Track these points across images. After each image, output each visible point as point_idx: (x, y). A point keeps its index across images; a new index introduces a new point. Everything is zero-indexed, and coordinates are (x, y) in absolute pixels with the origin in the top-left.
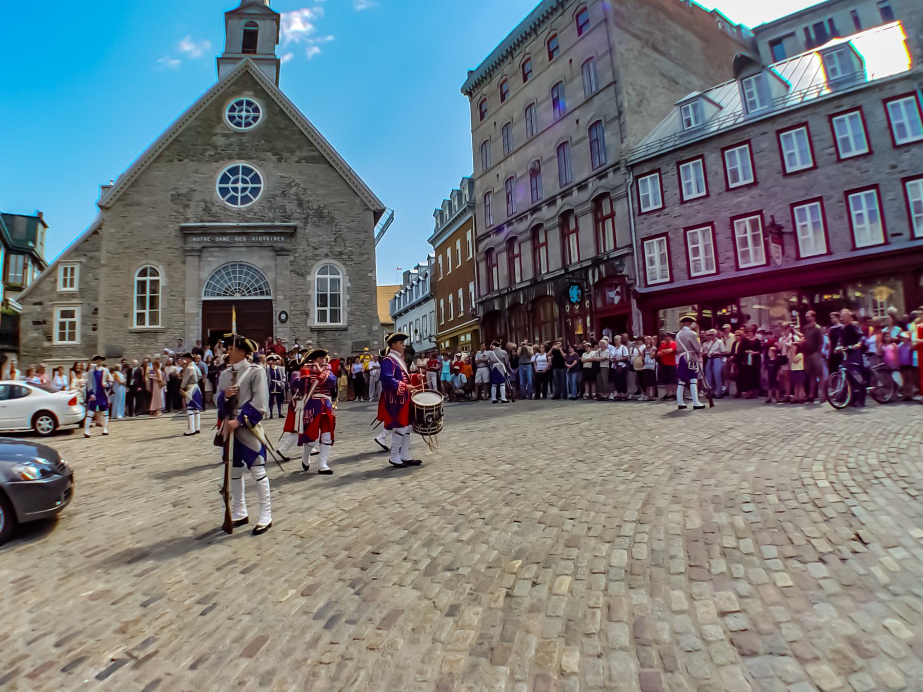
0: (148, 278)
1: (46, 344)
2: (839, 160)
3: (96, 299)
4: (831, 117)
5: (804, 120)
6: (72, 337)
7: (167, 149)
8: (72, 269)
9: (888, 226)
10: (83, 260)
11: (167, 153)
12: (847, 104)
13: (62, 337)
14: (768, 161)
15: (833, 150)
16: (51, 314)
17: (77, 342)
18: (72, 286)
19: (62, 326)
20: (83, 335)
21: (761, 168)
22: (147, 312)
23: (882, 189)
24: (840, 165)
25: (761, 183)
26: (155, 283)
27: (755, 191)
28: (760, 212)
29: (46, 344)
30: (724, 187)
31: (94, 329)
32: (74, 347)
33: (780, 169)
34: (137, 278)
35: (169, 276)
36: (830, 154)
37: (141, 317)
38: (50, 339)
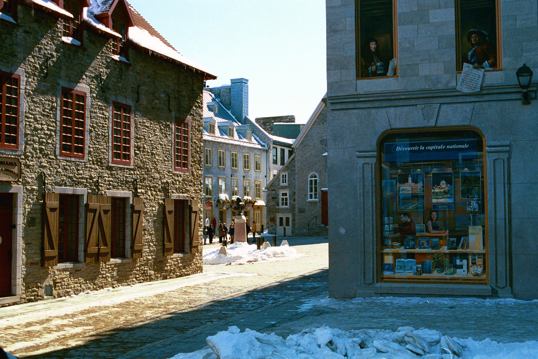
0: (313, 179)
1: (277, 207)
3: (294, 188)
6: (286, 204)
7: (317, 118)
8: (285, 175)
10: (290, 171)
11: (317, 120)
13: (283, 204)
16: (278, 195)
17: (288, 206)
18: (285, 182)
19: (283, 199)
20: (290, 203)
22: (313, 193)
26: (316, 181)
29: (277, 207)
31: (294, 201)
32: (287, 209)
34: (309, 179)
35: (320, 177)
37: (311, 195)
38: (278, 205)
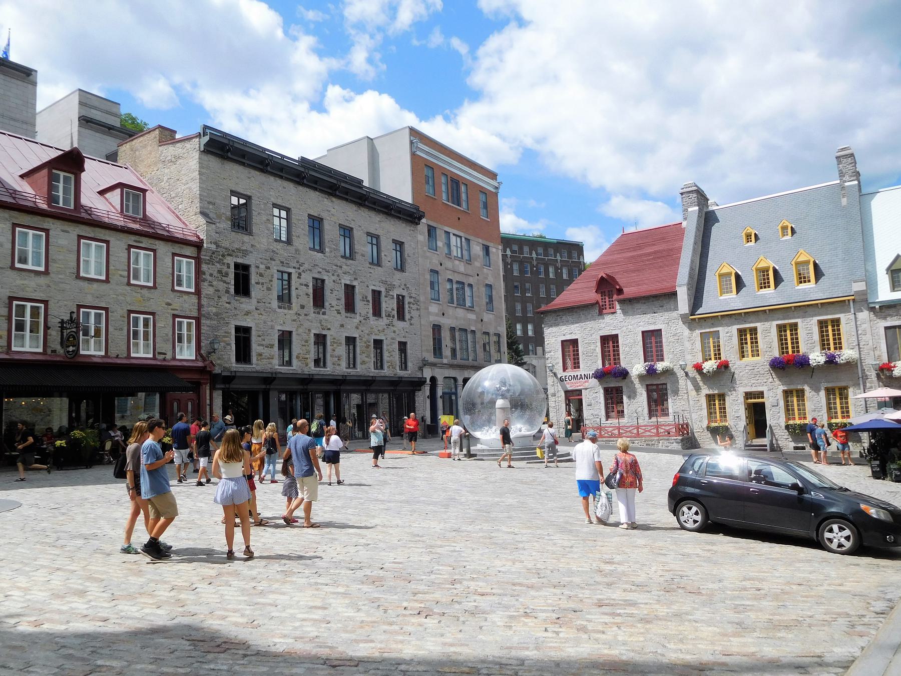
2: (129, 284)
4: (130, 246)
5: (108, 239)
9: (157, 345)
12: (146, 242)
14: (63, 259)
15: (126, 273)
21: (55, 261)
23: (157, 317)
24: (128, 288)
25: (52, 275)
27: (42, 280)
28: (45, 302)
30: (9, 263)
33: (75, 271)
36: (121, 276)
